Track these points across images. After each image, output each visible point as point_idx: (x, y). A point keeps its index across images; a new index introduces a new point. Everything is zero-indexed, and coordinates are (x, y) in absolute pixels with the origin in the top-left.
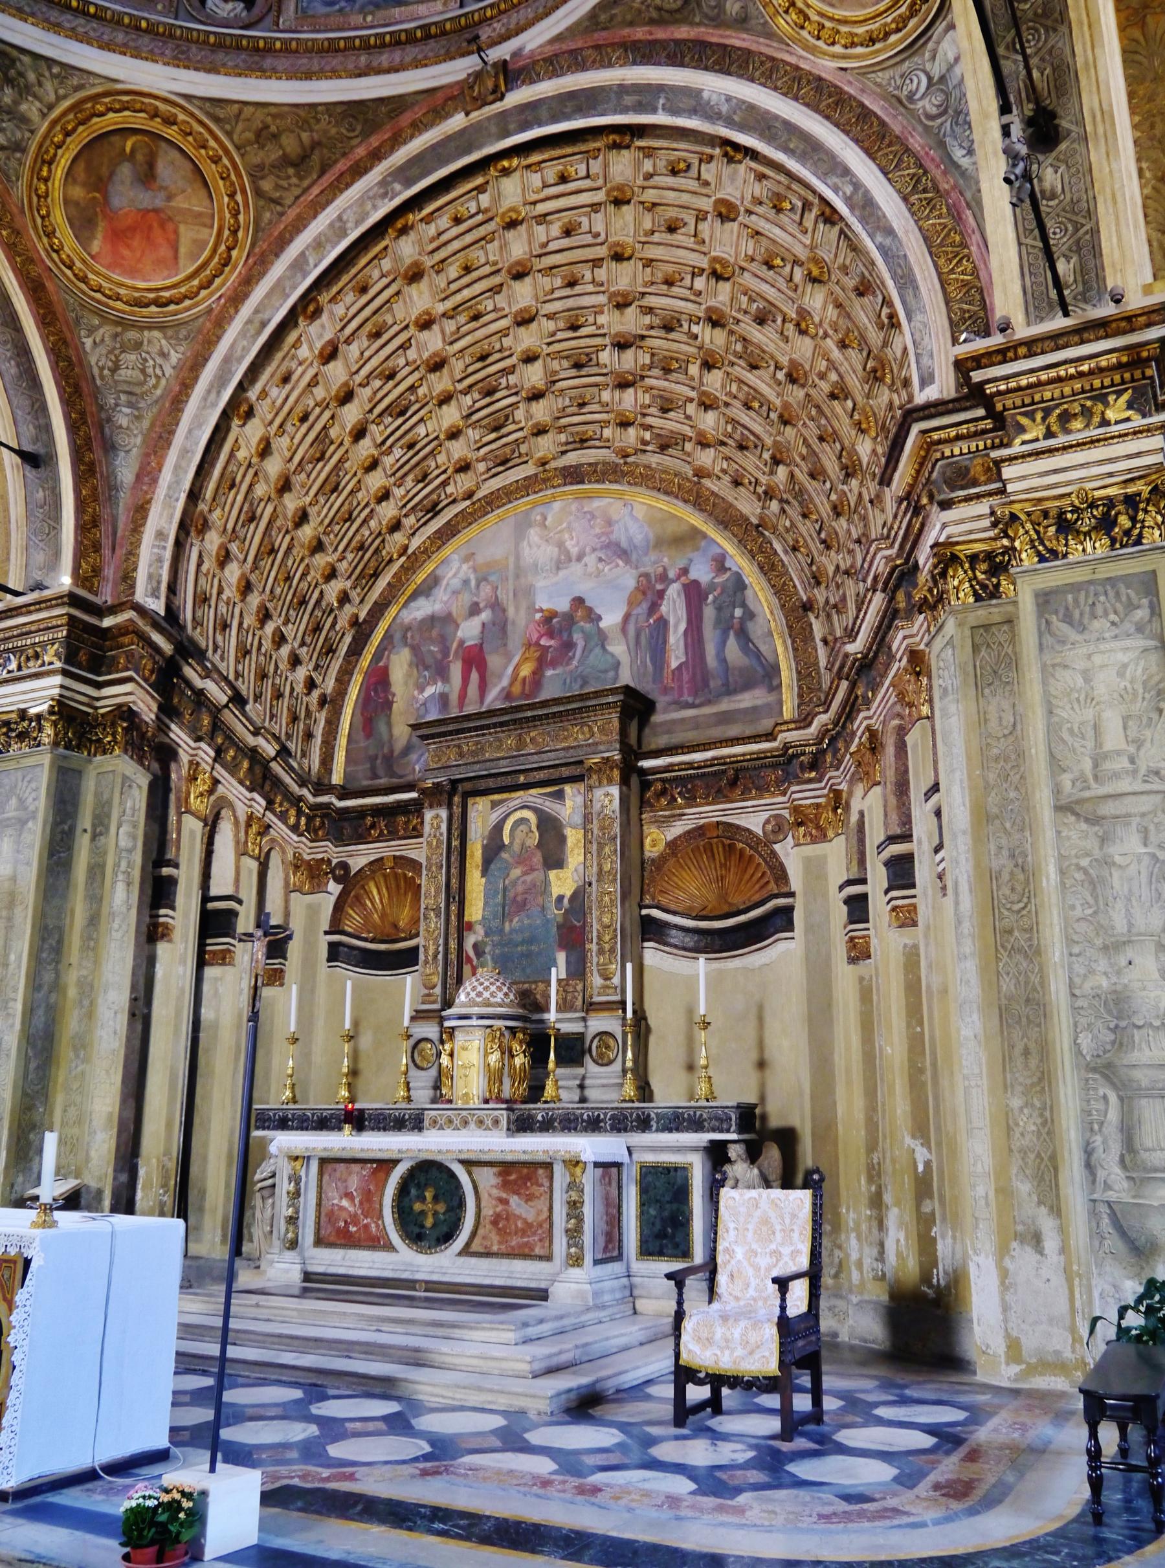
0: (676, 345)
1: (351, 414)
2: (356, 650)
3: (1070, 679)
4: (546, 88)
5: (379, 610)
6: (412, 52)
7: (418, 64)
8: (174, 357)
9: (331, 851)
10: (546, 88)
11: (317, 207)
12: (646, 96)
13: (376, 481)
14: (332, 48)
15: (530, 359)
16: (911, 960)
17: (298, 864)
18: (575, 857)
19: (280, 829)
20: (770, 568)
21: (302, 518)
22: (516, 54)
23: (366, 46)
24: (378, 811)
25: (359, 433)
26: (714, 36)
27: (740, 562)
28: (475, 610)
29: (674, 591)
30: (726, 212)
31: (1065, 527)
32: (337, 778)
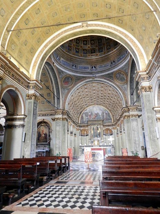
0: (105, 97)
1: (80, 97)
2: (80, 114)
3: (133, 124)
4: (98, 79)
5: (82, 111)
6: (88, 73)
7: (88, 74)
8: (67, 91)
9: (80, 128)
10: (98, 79)
11: (79, 83)
12: (105, 82)
13: (82, 102)
14: (82, 72)
15: (95, 96)
16: (122, 137)
17: (76, 129)
18: (99, 130)
19: (75, 126)
20: (111, 113)
21: (76, 104)
22: (95, 76)
23: (84, 72)
24: (83, 126)
25: (81, 99)
26: (110, 79)
27: (109, 112)
28: (90, 112)
29: (105, 113)
30: (110, 90)
31: (133, 116)
32: (79, 123)
